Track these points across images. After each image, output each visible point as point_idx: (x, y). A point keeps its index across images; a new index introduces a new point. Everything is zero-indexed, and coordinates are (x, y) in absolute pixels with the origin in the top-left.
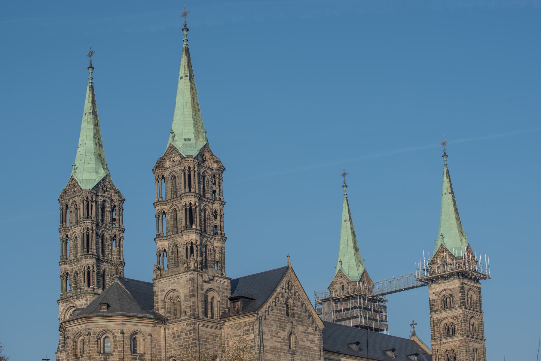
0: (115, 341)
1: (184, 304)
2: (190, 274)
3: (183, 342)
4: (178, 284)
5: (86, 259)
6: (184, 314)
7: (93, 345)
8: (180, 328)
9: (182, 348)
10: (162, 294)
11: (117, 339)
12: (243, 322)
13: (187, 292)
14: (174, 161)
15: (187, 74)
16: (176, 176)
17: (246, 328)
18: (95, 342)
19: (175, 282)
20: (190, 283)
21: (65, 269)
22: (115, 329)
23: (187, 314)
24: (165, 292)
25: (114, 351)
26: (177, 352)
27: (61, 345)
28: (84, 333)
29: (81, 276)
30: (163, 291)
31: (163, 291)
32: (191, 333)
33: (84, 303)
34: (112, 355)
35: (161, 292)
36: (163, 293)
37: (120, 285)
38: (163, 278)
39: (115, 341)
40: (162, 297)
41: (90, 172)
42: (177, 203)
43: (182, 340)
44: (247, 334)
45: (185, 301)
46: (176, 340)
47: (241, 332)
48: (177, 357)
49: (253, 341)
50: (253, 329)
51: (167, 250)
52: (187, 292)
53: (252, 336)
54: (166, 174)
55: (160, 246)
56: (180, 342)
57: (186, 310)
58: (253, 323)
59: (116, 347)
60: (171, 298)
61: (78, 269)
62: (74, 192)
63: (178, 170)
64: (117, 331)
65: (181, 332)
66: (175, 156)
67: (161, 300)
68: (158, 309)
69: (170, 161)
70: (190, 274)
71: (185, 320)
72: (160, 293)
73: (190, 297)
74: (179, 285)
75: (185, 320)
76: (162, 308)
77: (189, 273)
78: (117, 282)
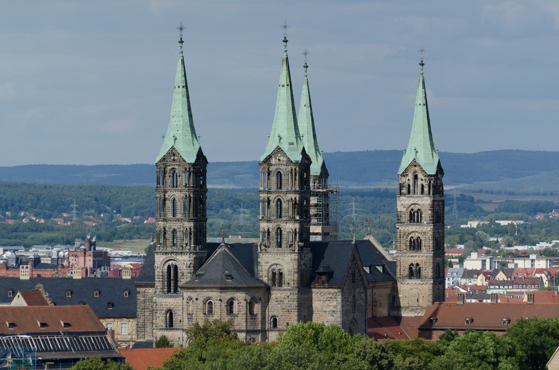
0: (239, 306)
1: (287, 277)
2: (294, 256)
3: (286, 306)
4: (282, 260)
5: (190, 223)
6: (288, 285)
7: (223, 308)
8: (283, 295)
9: (285, 310)
10: (266, 265)
11: (241, 304)
12: (327, 291)
13: (291, 269)
14: (279, 160)
15: (288, 84)
16: (282, 173)
17: (329, 296)
18: (225, 306)
19: (280, 259)
20: (294, 262)
21: (163, 225)
22: (240, 297)
23: (290, 285)
24: (269, 265)
25: (238, 314)
26: (280, 313)
27: (158, 290)
28: (215, 298)
29: (180, 234)
30: (267, 263)
31: (267, 263)
32: (294, 301)
33: (186, 260)
34: (238, 317)
35: (265, 263)
36: (267, 264)
37: (228, 253)
38: (268, 253)
39: (239, 306)
40: (267, 268)
41: (188, 144)
42: (282, 195)
43: (284, 304)
44: (330, 301)
45: (289, 275)
46: (279, 304)
47: (324, 298)
48: (280, 317)
49: (335, 307)
50: (336, 298)
51: (270, 230)
52: (291, 269)
53: (335, 303)
54: (272, 168)
55: (265, 226)
56: (283, 306)
57: (290, 282)
58: (337, 293)
59: (240, 310)
60: (273, 270)
61: (177, 228)
62: (174, 160)
63: (284, 169)
64: (241, 298)
65: (284, 298)
66: (281, 156)
67: (265, 270)
68: (262, 277)
69: (276, 159)
70: (294, 256)
71: (289, 290)
72: (264, 264)
73: (294, 273)
74: (283, 261)
75: (289, 290)
76: (265, 276)
77: (294, 254)
78: (224, 250)
